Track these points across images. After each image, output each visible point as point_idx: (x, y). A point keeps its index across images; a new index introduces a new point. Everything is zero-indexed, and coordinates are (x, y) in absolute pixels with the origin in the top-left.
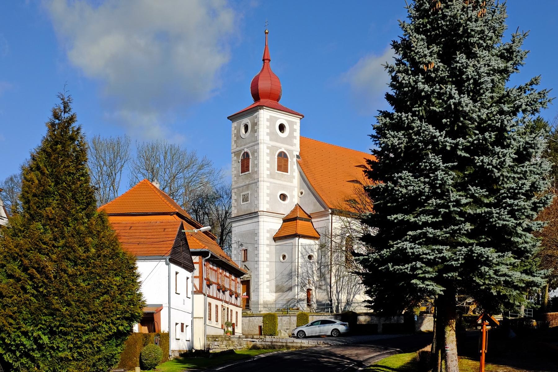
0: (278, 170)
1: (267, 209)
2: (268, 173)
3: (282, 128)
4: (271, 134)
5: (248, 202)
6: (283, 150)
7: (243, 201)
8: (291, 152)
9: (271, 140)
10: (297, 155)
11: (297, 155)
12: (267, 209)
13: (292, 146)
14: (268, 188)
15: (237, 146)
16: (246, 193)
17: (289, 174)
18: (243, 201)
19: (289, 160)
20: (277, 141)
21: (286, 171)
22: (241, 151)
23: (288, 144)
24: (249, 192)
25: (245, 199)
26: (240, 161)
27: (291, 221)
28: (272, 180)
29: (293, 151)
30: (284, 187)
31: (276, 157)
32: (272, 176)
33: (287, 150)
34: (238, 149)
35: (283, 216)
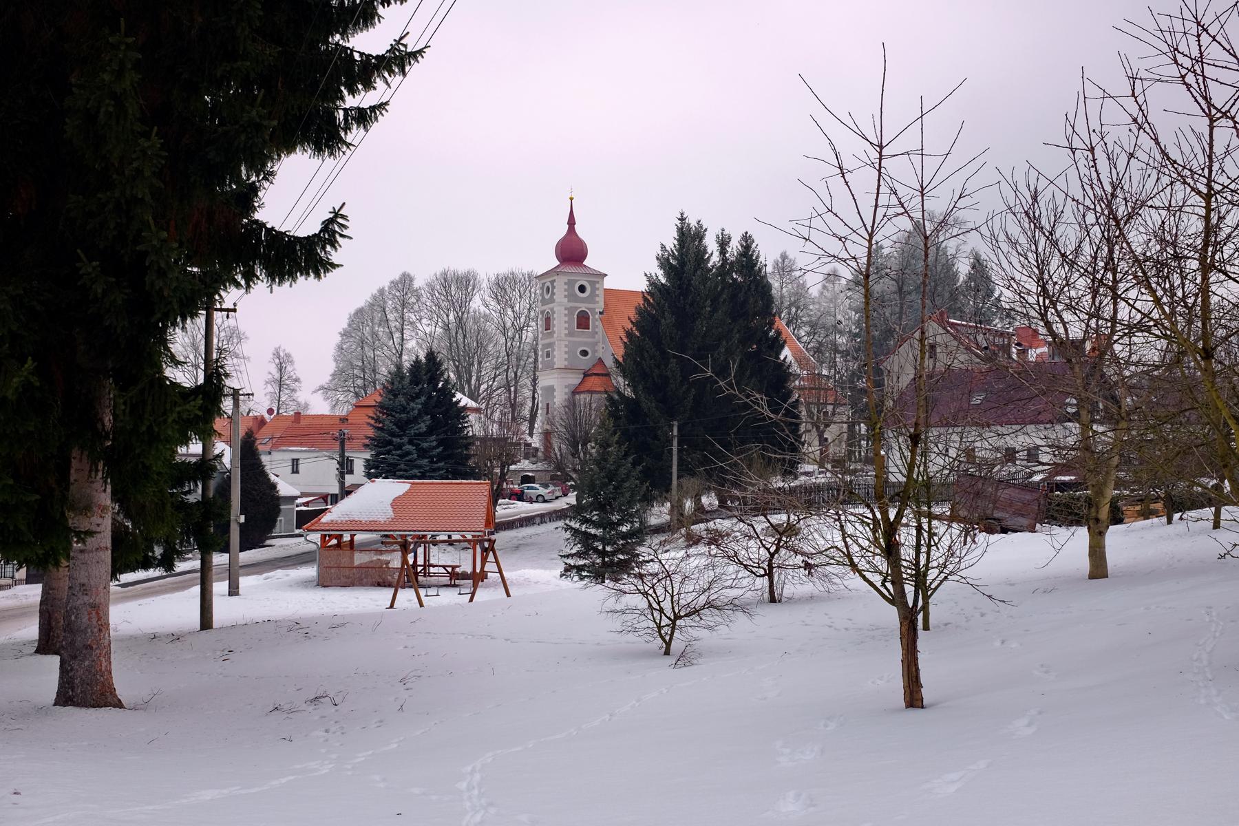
2: (567, 332)
6: (584, 309)
8: (592, 310)
14: (566, 346)
19: (591, 317)
28: (571, 339)
29: (595, 309)
30: (585, 344)
31: (576, 316)
32: (571, 334)
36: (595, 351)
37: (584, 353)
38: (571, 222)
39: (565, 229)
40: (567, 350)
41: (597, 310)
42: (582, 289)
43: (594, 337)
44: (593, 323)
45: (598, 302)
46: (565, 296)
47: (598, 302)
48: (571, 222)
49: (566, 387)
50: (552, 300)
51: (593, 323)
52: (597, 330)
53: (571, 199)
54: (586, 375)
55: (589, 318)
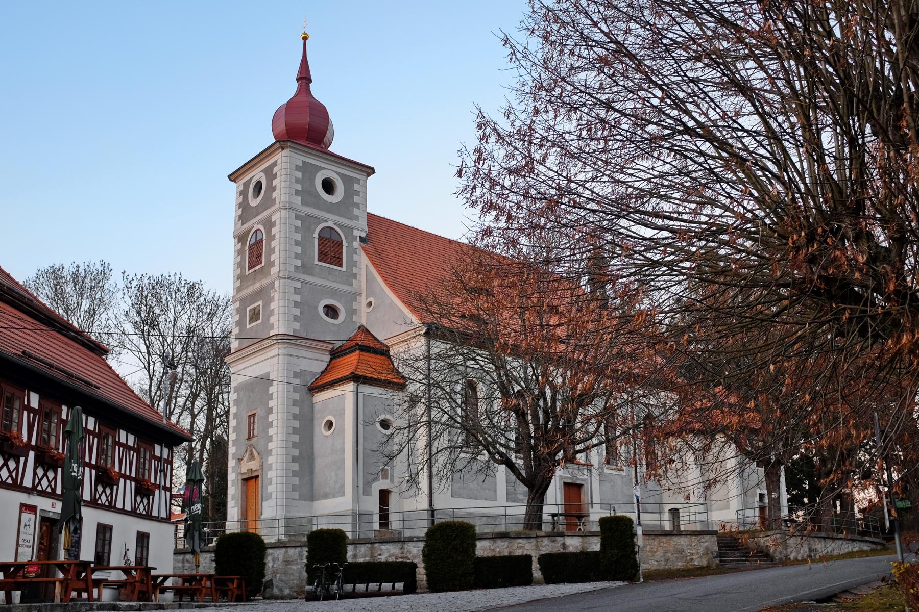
0: (319, 260)
1: (294, 330)
2: (298, 263)
3: (328, 186)
4: (307, 195)
5: (258, 322)
6: (330, 224)
7: (251, 321)
8: (349, 230)
9: (304, 203)
10: (360, 237)
11: (360, 237)
12: (294, 330)
13: (351, 219)
15: (242, 224)
16: (256, 305)
17: (344, 269)
18: (251, 321)
19: (345, 244)
20: (318, 208)
21: (338, 261)
22: (249, 231)
23: (342, 216)
24: (260, 303)
25: (255, 316)
26: (247, 248)
27: (347, 354)
29: (351, 229)
30: (334, 293)
31: (316, 235)
32: (305, 268)
33: (341, 226)
34: (246, 226)
35: (332, 346)
36: (352, 312)
37: (332, 311)
38: (304, 78)
39: (290, 89)
40: (298, 298)
41: (357, 233)
42: (328, 186)
43: (351, 285)
44: (350, 257)
45: (357, 218)
46: (297, 193)
47: (357, 218)
48: (304, 78)
49: (296, 375)
50: (268, 202)
51: (350, 257)
52: (355, 270)
53: (305, 39)
54: (336, 354)
55: (340, 244)
